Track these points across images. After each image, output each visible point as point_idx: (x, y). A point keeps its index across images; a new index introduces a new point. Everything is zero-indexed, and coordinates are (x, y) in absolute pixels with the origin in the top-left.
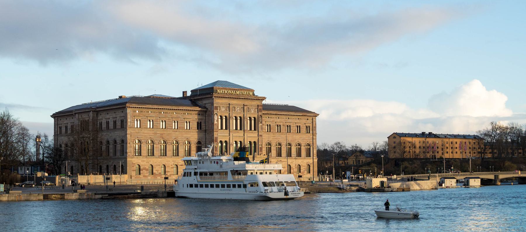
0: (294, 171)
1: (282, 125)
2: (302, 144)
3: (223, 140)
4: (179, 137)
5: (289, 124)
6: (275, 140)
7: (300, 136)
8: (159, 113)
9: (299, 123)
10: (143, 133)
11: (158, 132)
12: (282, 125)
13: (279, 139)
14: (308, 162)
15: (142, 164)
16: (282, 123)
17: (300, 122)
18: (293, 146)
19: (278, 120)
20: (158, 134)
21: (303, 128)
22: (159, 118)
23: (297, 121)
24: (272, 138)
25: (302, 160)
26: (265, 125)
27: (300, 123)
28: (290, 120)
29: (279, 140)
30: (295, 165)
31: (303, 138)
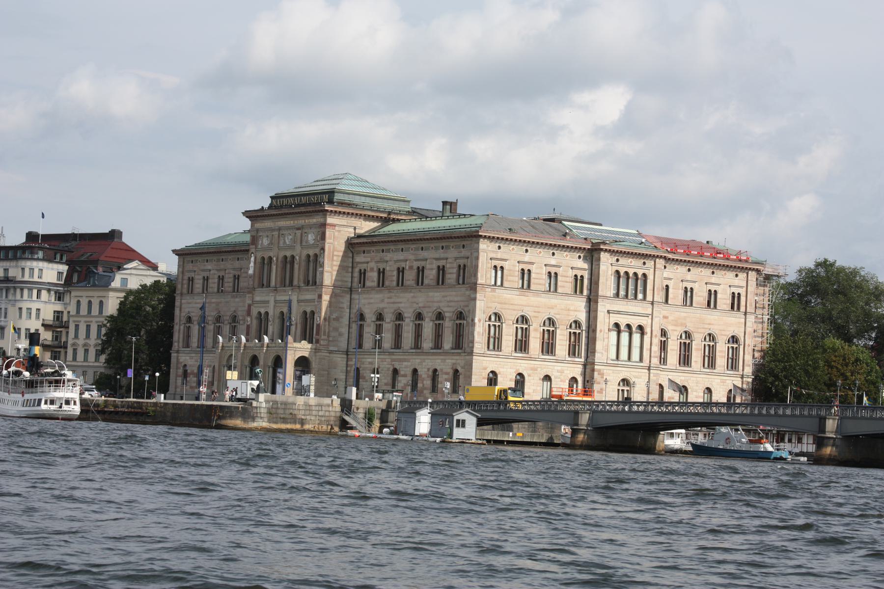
0: (423, 385)
1: (407, 268)
2: (447, 315)
3: (263, 311)
4: (240, 309)
5: (421, 264)
6: (392, 305)
7: (443, 294)
8: (217, 262)
9: (443, 259)
10: (196, 303)
11: (213, 300)
12: (407, 268)
13: (401, 303)
14: (454, 361)
15: (190, 363)
16: (408, 263)
17: (445, 255)
18: (427, 320)
19: (401, 256)
20: (213, 303)
21: (450, 271)
22: (216, 272)
23: (441, 253)
24: (386, 300)
25: (442, 357)
26: (375, 269)
27: (447, 259)
28: (425, 254)
29: (400, 305)
30: (426, 370)
31: (448, 299)
